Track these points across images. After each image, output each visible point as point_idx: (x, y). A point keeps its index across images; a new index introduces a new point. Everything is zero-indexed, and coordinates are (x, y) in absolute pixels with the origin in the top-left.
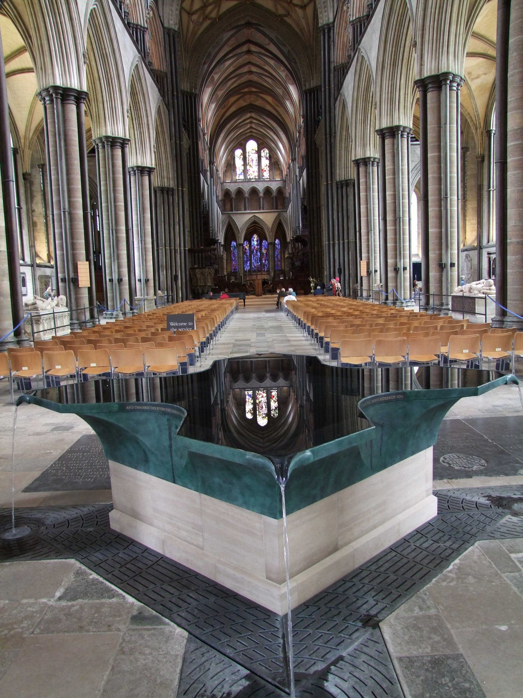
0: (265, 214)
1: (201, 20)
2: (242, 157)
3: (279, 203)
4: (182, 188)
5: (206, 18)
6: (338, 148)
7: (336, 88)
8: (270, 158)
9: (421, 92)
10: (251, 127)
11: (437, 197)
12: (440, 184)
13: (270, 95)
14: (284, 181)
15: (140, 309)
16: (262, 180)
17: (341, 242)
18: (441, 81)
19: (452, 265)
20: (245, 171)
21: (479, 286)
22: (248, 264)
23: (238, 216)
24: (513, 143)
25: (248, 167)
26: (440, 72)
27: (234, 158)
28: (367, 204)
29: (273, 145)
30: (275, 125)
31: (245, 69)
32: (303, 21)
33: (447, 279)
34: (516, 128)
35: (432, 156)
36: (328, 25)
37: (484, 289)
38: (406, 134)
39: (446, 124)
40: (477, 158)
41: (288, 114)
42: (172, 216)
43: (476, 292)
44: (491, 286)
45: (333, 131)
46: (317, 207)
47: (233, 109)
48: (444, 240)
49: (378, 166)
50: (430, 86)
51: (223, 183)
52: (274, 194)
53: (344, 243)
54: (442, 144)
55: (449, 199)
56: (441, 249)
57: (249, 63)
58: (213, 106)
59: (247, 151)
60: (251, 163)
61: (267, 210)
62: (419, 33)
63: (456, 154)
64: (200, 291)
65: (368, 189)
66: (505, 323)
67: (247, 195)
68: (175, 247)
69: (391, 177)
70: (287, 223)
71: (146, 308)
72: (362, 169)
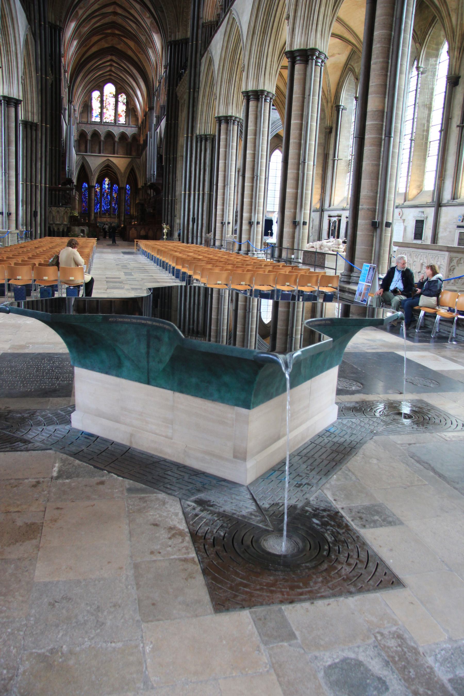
2: (99, 99)
4: (46, 124)
6: (200, 103)
7: (203, 45)
9: (290, 63)
10: (111, 71)
11: (296, 161)
12: (300, 150)
15: (3, 242)
16: (117, 125)
17: (197, 193)
18: (308, 56)
19: (304, 223)
20: (101, 114)
21: (330, 244)
23: (92, 158)
24: (371, 123)
25: (105, 111)
26: (308, 47)
27: (91, 99)
28: (225, 160)
30: (135, 71)
33: (299, 235)
34: (374, 110)
35: (295, 123)
37: (334, 247)
38: (269, 98)
39: (309, 95)
40: (326, 128)
41: (149, 61)
42: (34, 151)
43: (327, 249)
44: (339, 245)
45: (197, 86)
46: (173, 158)
48: (299, 201)
49: (238, 125)
50: (298, 58)
51: (80, 123)
52: (130, 140)
54: (304, 113)
55: (306, 164)
56: (295, 208)
59: (105, 94)
60: (108, 106)
62: (293, 7)
63: (315, 124)
64: (56, 229)
65: (227, 146)
66: (352, 278)
67: (102, 138)
68: (36, 183)
69: (252, 137)
71: (9, 241)
72: (223, 126)
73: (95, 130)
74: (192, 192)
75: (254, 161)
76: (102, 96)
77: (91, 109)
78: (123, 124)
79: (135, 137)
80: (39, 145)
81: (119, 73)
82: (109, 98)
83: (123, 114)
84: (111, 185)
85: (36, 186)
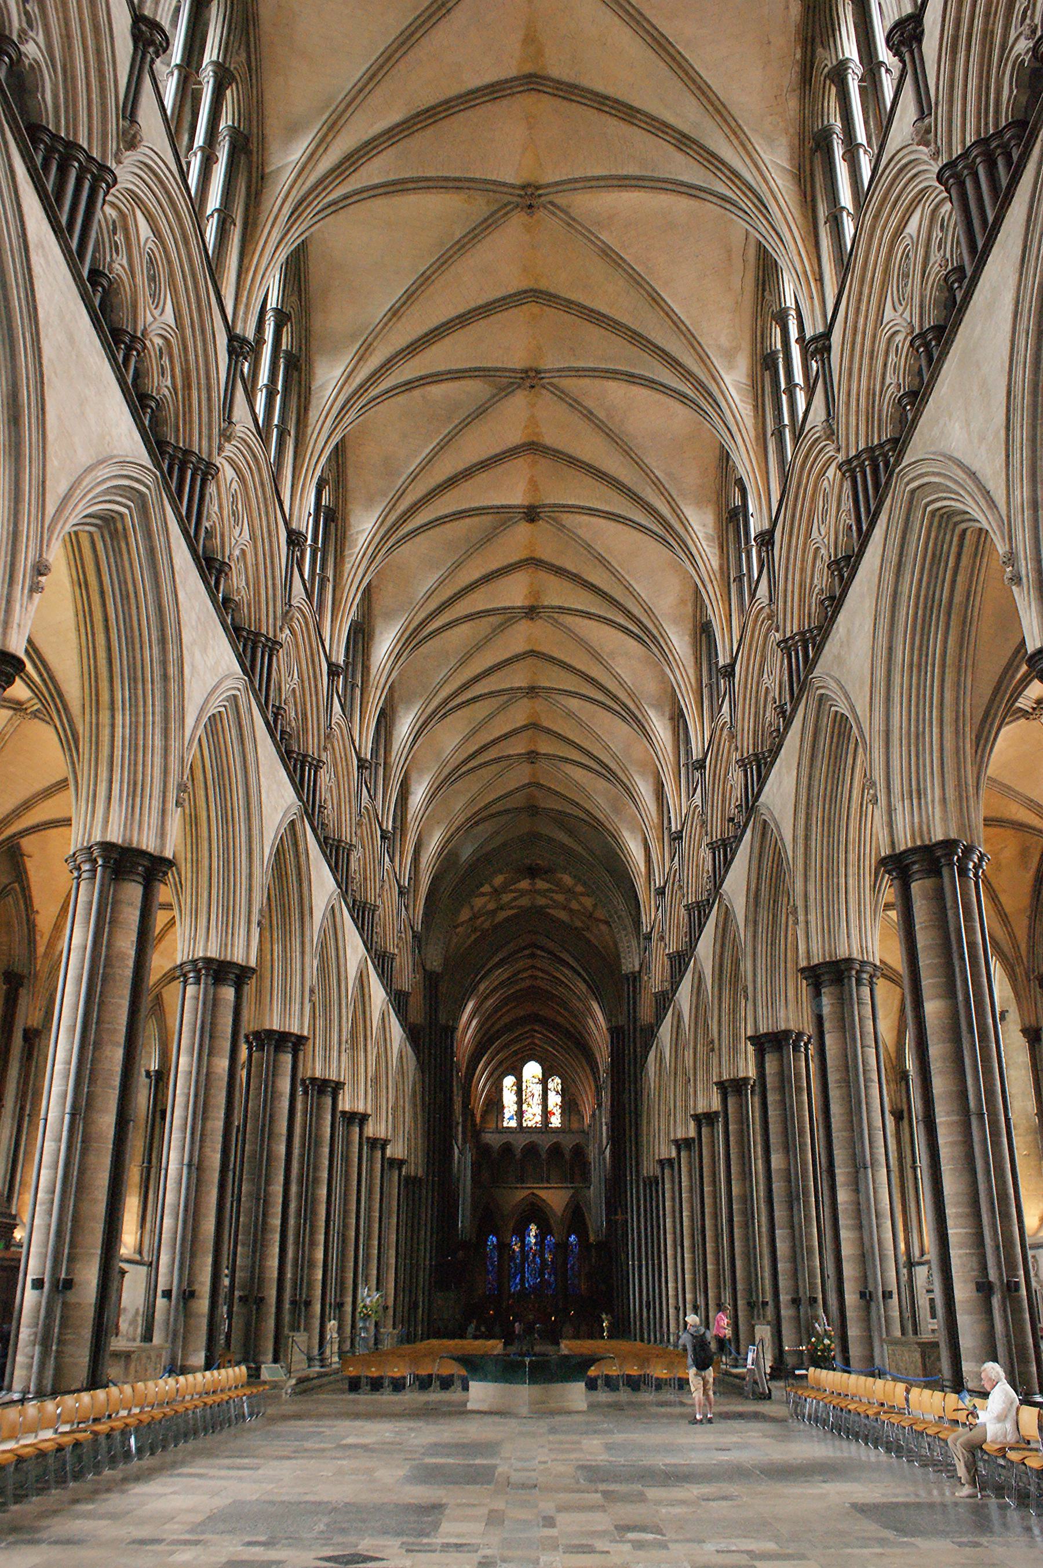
2: (515, 1088)
5: (475, 930)
8: (564, 1093)
12: (716, 1220)
13: (565, 1009)
20: (520, 1114)
22: (517, 1280)
25: (525, 1107)
27: (500, 1090)
31: (529, 972)
52: (567, 1157)
53: (653, 1265)
57: (533, 967)
58: (474, 1023)
59: (524, 1080)
60: (530, 1100)
62: (692, 1072)
67: (518, 1156)
70: (590, 1209)
77: (503, 1107)
83: (557, 1111)
84: (541, 1237)
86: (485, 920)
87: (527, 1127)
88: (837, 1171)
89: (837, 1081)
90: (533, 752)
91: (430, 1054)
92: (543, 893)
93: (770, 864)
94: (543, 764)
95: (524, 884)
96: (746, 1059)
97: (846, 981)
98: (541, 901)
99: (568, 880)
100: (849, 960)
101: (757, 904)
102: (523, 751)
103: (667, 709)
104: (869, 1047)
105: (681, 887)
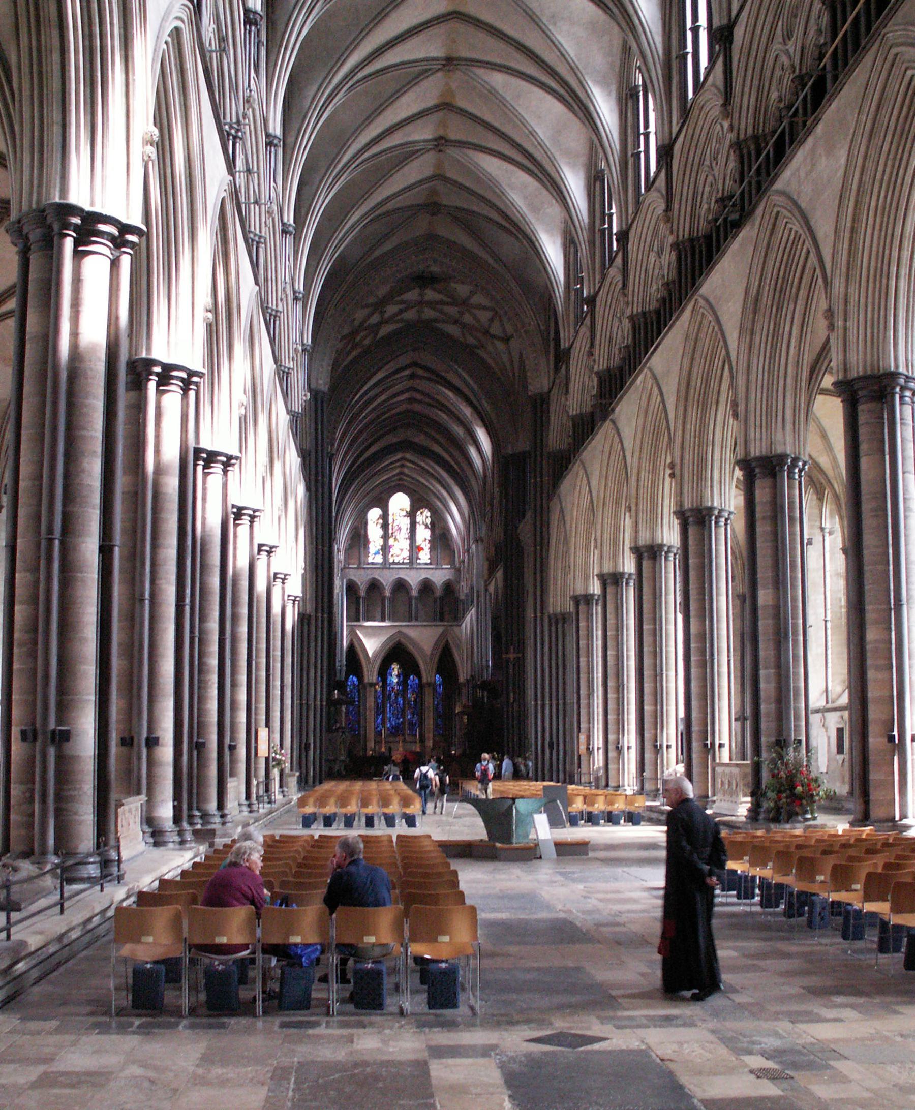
0: (419, 629)
1: (349, 348)
2: (381, 521)
3: (446, 609)
8: (433, 527)
10: (401, 473)
14: (458, 571)
20: (385, 549)
25: (391, 541)
27: (366, 523)
29: (439, 503)
30: (445, 475)
32: (505, 358)
36: (541, 395)
39: (661, 595)
47: (373, 450)
51: (345, 568)
52: (439, 593)
53: (557, 705)
59: (391, 512)
61: (424, 621)
69: (614, 633)
72: (582, 607)
73: (374, 579)
74: (547, 702)
75: (618, 664)
76: (385, 517)
77: (366, 542)
78: (426, 564)
79: (449, 588)
80: (312, 645)
81: (415, 475)
82: (398, 518)
83: (426, 546)
85: (307, 704)
86: (366, 337)
87: (394, 563)
88: (869, 608)
89: (872, 510)
90: (441, 138)
91: (316, 481)
92: (431, 304)
93: (777, 264)
94: (453, 152)
95: (412, 295)
96: (712, 487)
97: (889, 398)
98: (429, 313)
99: (463, 290)
100: (894, 375)
101: (755, 312)
102: (430, 137)
103: (614, 88)
104: (909, 472)
105: (625, 295)
